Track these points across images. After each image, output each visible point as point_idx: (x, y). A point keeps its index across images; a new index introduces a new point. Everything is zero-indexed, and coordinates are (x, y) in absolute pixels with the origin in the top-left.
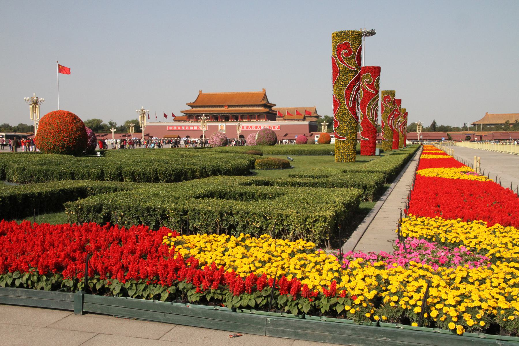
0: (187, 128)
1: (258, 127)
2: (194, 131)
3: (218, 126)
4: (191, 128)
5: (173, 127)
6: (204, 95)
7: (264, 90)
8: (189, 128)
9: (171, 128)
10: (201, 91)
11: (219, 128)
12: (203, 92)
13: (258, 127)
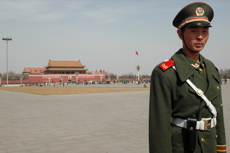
0: (53, 77)
4: (55, 77)
7: (79, 61)
9: (44, 78)
11: (69, 77)
12: (51, 60)
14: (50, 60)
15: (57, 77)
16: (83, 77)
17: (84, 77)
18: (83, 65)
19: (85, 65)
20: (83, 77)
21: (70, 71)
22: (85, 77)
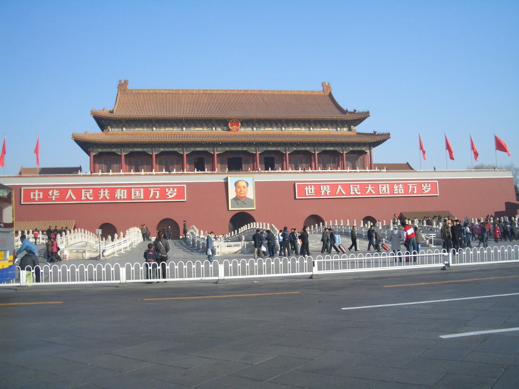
0: (104, 194)
1: (370, 188)
2: (130, 205)
3: (226, 184)
4: (121, 195)
5: (46, 192)
6: (137, 94)
8: (112, 191)
9: (37, 196)
10: (126, 82)
11: (232, 194)
12: (130, 87)
13: (370, 188)
14: (122, 86)
15: (138, 195)
16: (347, 187)
17: (355, 191)
18: (351, 110)
19: (361, 109)
20: (347, 187)
21: (252, 150)
22: (363, 187)
